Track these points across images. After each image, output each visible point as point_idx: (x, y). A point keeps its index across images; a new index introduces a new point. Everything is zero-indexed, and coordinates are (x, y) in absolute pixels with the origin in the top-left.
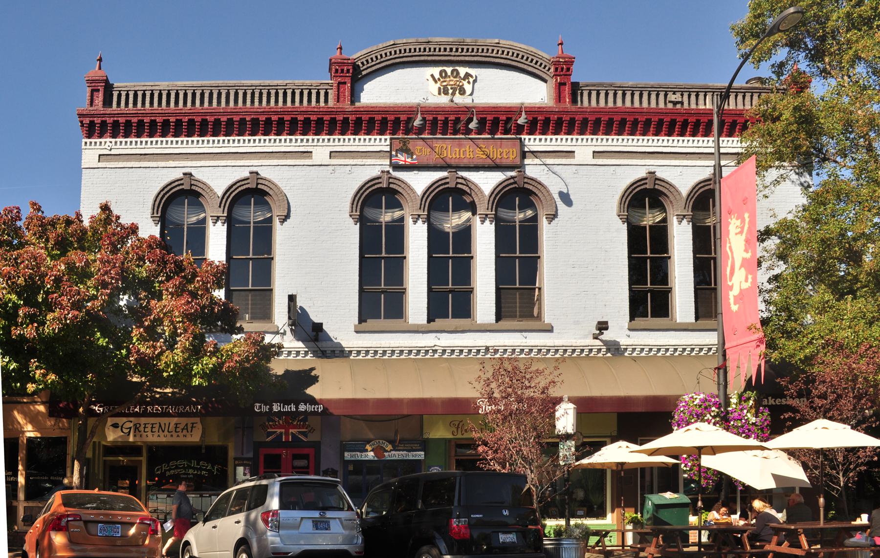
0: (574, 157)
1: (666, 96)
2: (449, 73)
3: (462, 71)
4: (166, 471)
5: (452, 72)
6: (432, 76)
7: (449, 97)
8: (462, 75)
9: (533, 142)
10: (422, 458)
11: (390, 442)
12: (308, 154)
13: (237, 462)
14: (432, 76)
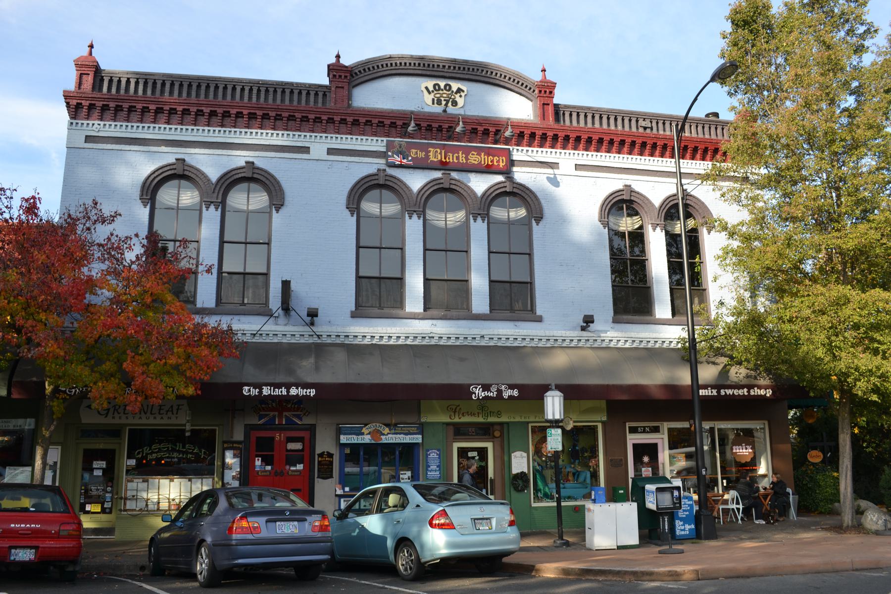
0: (558, 168)
1: (637, 121)
2: (442, 87)
3: (455, 86)
4: (147, 454)
5: (446, 86)
6: (427, 88)
7: (442, 107)
8: (454, 89)
9: (519, 153)
10: (420, 441)
11: (387, 425)
12: (306, 150)
13: (226, 445)
14: (427, 88)
